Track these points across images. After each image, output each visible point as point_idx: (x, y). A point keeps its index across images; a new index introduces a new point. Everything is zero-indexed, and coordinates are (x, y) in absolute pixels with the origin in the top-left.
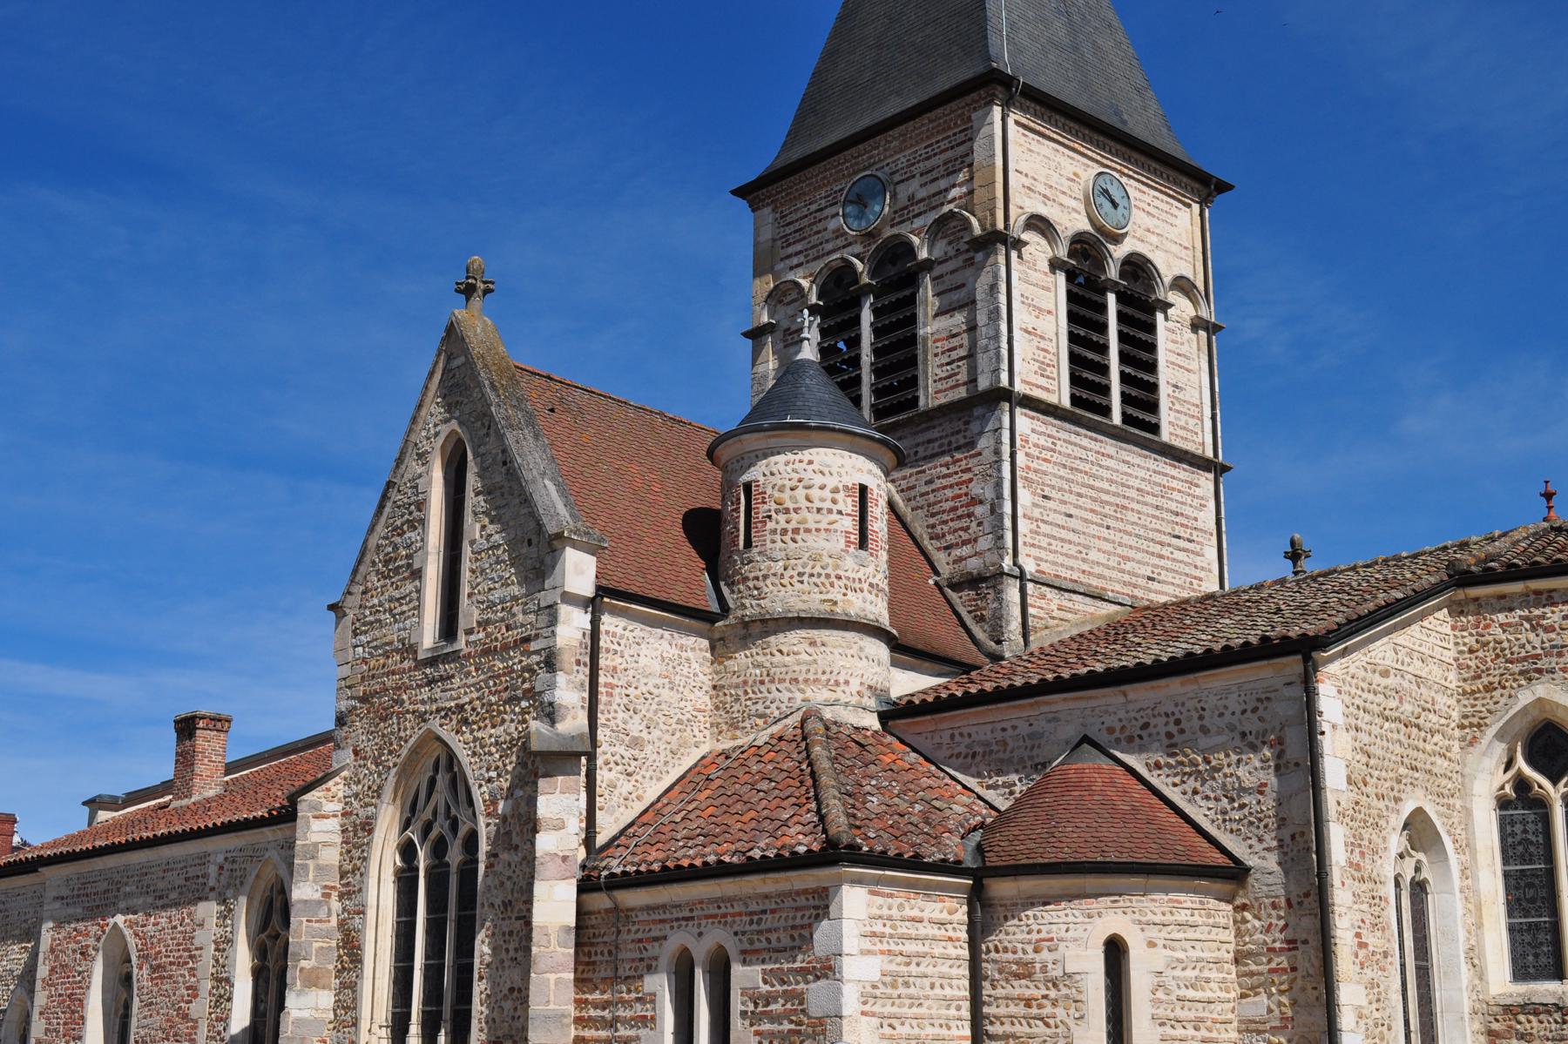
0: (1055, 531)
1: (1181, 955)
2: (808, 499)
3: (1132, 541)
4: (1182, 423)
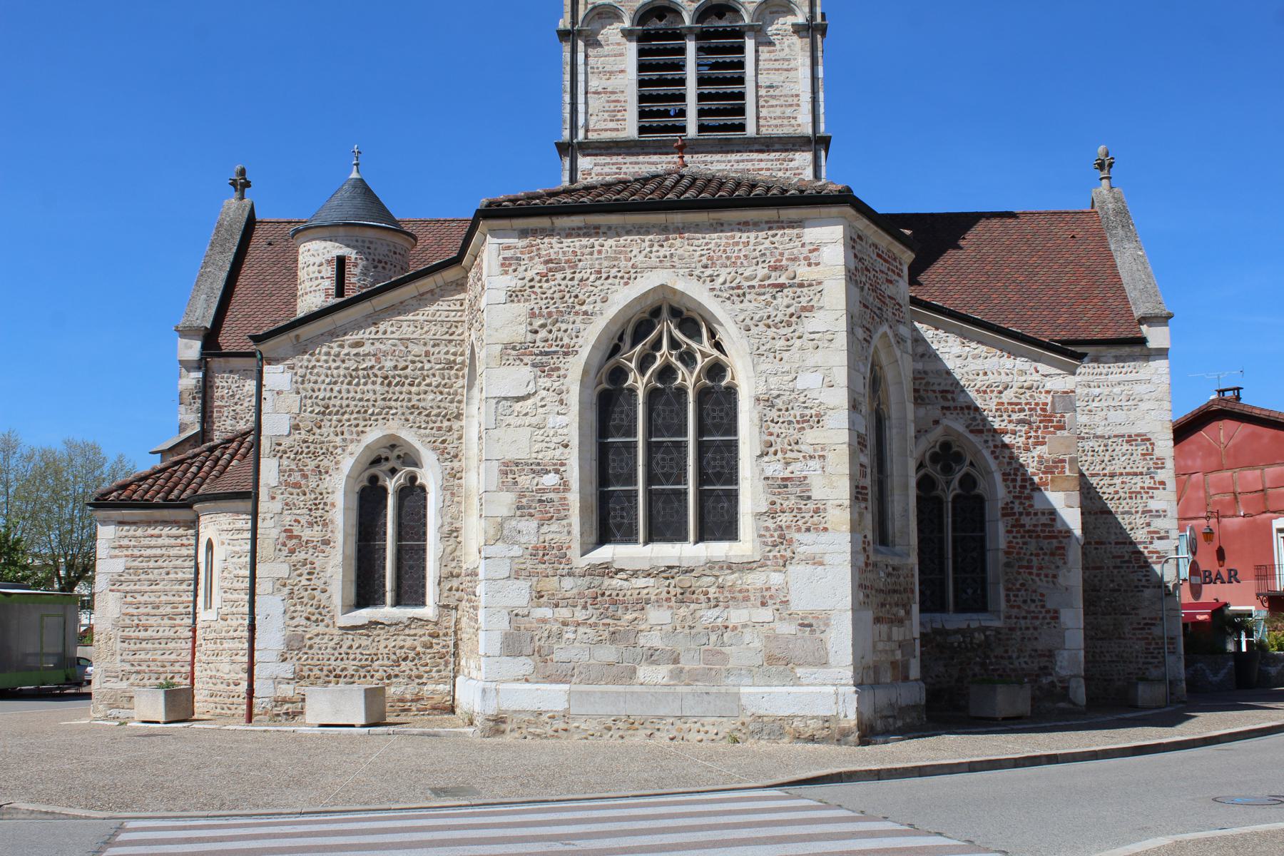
1: (237, 548)
4: (778, 114)
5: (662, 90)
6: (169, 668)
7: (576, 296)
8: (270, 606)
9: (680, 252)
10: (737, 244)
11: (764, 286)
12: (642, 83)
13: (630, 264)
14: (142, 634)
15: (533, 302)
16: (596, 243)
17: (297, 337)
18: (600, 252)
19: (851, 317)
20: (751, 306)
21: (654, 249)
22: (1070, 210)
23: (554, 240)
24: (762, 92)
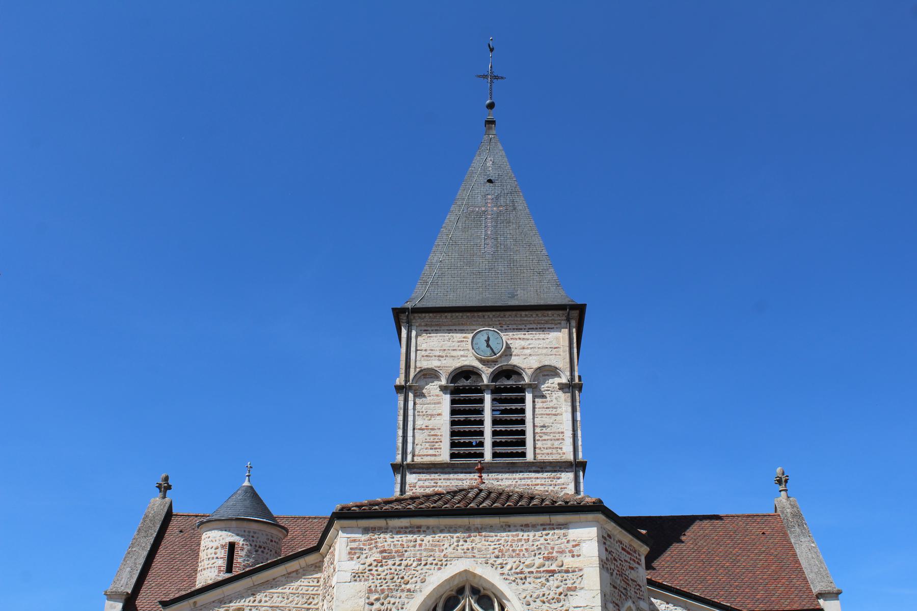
5: (467, 428)
7: (403, 578)
9: (479, 546)
10: (520, 540)
11: (540, 572)
12: (453, 423)
13: (442, 554)
15: (371, 581)
16: (418, 539)
17: (195, 603)
18: (420, 545)
19: (604, 595)
20: (531, 587)
21: (460, 543)
22: (760, 513)
23: (388, 536)
24: (538, 430)
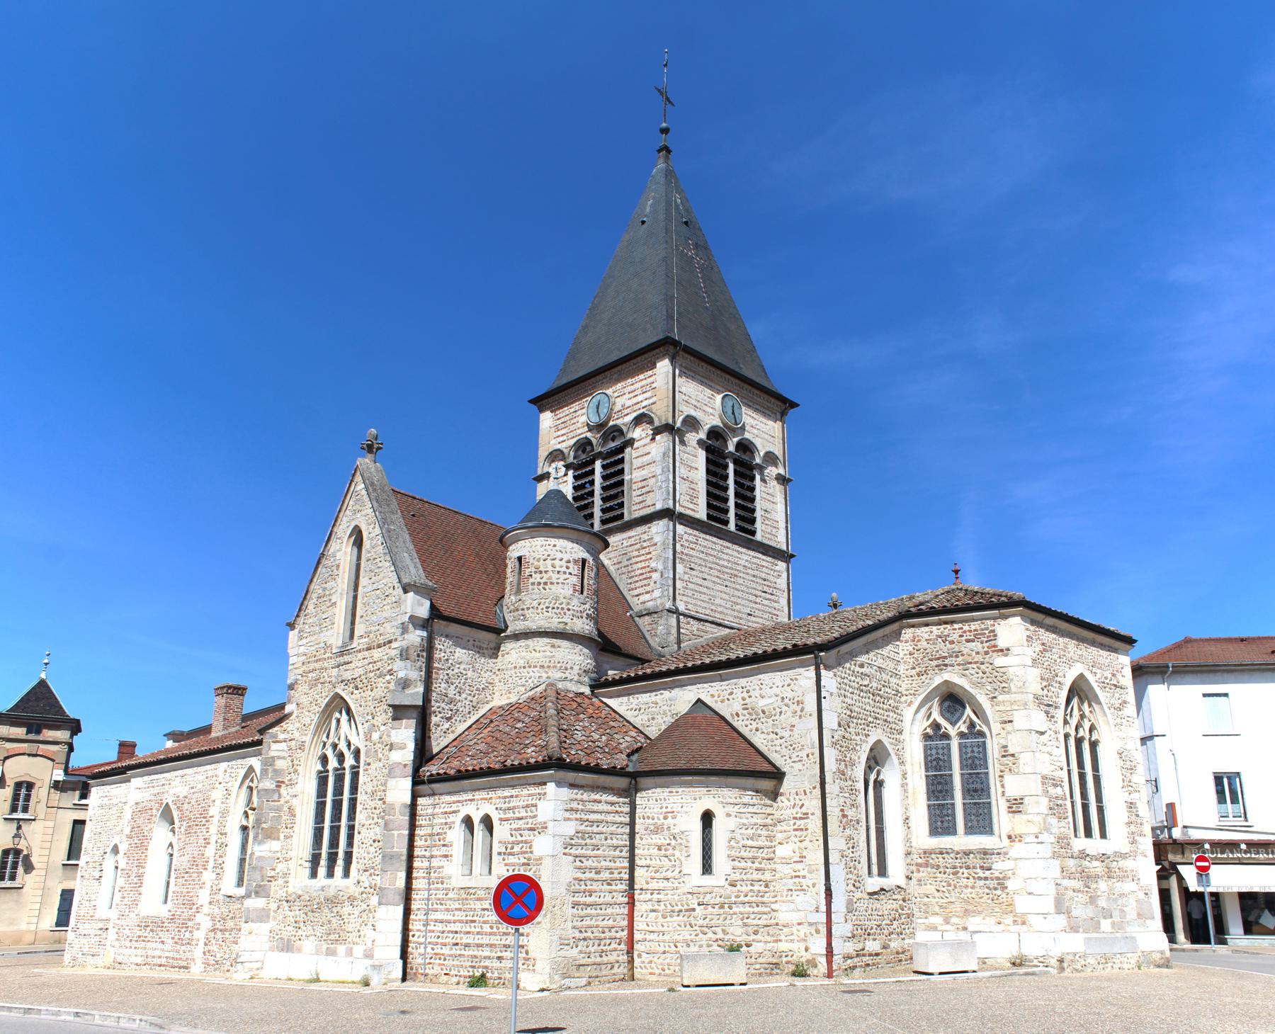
0: (697, 588)
1: (745, 821)
2: (553, 566)
3: (739, 594)
6: (607, 934)
8: (837, 873)
14: (588, 900)
